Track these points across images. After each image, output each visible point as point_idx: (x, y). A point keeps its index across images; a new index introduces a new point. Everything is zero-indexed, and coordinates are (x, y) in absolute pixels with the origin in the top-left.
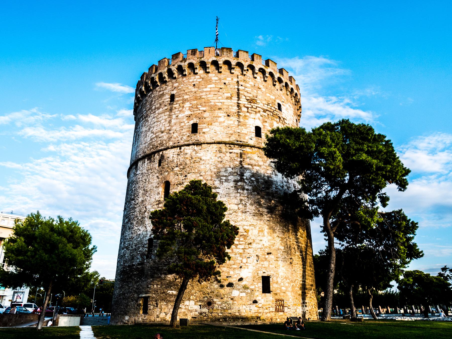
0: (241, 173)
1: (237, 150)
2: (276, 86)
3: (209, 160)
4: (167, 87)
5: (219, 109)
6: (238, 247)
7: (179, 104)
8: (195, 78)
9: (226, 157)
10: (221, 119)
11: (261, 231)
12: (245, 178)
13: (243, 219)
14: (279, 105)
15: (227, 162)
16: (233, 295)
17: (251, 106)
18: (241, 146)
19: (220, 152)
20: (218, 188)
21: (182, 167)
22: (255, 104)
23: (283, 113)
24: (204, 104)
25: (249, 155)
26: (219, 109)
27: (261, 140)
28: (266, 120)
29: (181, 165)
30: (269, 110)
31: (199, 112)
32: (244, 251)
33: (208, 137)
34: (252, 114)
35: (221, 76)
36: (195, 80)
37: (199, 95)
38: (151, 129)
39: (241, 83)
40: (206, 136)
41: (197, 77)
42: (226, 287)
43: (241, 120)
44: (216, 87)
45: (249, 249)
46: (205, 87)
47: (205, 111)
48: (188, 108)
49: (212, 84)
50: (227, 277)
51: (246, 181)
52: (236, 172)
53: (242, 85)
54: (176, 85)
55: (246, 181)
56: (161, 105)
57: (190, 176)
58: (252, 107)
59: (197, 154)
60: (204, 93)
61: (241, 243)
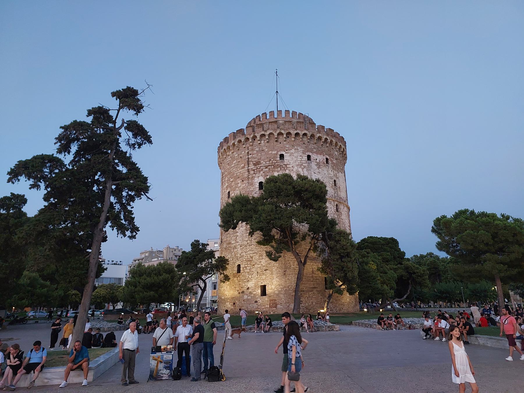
6: (247, 268)
16: (244, 298)
23: (285, 161)
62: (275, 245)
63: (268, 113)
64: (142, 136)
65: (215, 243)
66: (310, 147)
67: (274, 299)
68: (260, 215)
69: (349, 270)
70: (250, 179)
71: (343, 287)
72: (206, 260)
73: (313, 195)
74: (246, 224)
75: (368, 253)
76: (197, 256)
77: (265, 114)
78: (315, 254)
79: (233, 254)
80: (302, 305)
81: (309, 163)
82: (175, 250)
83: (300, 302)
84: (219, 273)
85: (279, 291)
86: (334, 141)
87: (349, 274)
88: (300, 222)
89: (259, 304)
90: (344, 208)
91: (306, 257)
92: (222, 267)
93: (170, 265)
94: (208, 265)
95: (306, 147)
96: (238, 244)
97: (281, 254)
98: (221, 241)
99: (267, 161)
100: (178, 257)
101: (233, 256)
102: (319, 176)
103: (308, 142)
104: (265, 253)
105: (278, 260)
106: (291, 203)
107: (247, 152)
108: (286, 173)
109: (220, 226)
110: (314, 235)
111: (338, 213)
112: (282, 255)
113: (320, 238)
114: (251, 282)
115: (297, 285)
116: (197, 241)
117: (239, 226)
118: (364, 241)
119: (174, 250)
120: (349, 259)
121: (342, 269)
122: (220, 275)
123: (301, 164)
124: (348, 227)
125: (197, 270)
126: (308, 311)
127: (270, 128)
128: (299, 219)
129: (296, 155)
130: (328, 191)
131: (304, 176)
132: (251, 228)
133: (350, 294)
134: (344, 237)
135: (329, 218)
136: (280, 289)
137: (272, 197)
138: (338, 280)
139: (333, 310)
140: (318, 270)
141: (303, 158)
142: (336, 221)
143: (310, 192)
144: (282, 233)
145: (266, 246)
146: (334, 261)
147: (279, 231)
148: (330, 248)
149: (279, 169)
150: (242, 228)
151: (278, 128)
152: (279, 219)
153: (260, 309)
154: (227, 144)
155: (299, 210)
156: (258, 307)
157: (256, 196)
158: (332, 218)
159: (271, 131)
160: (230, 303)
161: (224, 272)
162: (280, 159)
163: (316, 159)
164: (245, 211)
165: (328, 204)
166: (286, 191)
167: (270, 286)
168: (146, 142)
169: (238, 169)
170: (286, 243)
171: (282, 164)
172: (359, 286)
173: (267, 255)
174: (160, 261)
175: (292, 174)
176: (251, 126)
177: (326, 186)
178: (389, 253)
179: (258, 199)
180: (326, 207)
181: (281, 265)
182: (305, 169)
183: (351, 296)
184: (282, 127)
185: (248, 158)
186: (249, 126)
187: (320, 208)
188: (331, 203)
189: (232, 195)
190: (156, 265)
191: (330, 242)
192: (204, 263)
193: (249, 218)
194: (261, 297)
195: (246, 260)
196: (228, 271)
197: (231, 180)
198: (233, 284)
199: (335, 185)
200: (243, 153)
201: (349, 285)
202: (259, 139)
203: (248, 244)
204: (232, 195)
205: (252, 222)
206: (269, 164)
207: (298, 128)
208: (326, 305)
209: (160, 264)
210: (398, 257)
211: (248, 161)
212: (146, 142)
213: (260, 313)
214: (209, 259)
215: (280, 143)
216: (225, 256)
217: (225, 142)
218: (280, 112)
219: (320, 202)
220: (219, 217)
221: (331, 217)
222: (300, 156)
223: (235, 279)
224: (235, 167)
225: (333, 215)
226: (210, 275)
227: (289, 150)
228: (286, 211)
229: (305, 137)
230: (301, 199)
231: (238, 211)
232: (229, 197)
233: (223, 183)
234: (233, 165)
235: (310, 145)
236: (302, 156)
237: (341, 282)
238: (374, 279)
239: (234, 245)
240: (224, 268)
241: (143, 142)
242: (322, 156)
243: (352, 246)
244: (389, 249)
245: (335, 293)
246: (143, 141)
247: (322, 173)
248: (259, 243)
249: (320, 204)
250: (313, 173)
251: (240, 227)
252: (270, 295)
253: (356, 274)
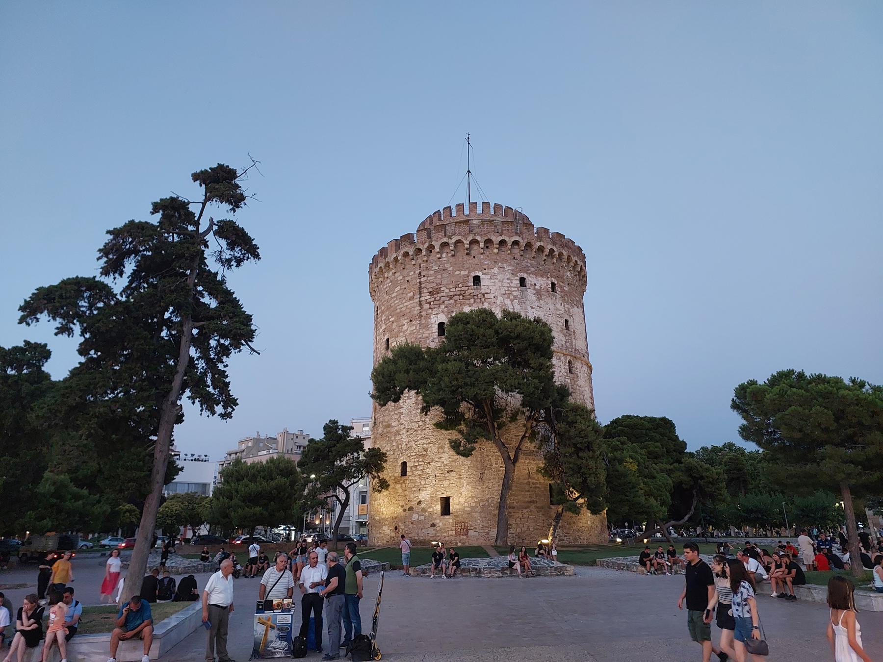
11: (442, 447)
16: (413, 519)
22: (439, 295)
23: (482, 287)
62: (465, 429)
63: (453, 207)
64: (243, 245)
65: (364, 425)
66: (524, 264)
67: (463, 520)
68: (440, 379)
69: (591, 472)
70: (423, 318)
71: (581, 501)
72: (350, 454)
73: (529, 345)
74: (417, 393)
75: (623, 444)
76: (334, 447)
77: (449, 208)
78: (533, 445)
79: (394, 444)
80: (512, 531)
81: (522, 291)
82: (297, 437)
83: (508, 527)
84: (370, 477)
85: (472, 507)
86: (565, 253)
87: (591, 480)
88: (508, 391)
89: (438, 529)
90: (582, 367)
91: (518, 449)
92: (375, 466)
93: (289, 462)
94: (353, 463)
95: (518, 264)
96: (403, 426)
97: (475, 445)
98: (375, 423)
99: (452, 287)
100: (302, 449)
101: (395, 448)
102: (539, 313)
103: (521, 256)
104: (448, 442)
105: (471, 455)
106: (492, 359)
107: (417, 272)
108: (483, 307)
109: (372, 396)
110: (532, 412)
111: (572, 376)
112: (477, 446)
113: (542, 417)
114: (425, 492)
115: (503, 497)
116: (335, 422)
117: (405, 397)
118: (616, 422)
119: (295, 436)
120: (591, 453)
121: (578, 470)
122: (372, 480)
123: (509, 292)
124: (590, 400)
125: (334, 471)
126: (521, 541)
127: (457, 233)
128: (506, 385)
129: (500, 277)
130: (554, 338)
131: (514, 312)
132: (425, 401)
133: (592, 513)
134: (583, 417)
135: (556, 384)
136: (474, 505)
137: (460, 348)
138: (571, 489)
139: (564, 540)
140: (538, 471)
141: (512, 283)
142: (568, 388)
143: (524, 340)
144: (477, 410)
145: (450, 432)
146: (565, 456)
147: (471, 406)
148: (559, 435)
149: (472, 301)
150: (409, 400)
151: (471, 231)
152: (472, 385)
153: (439, 538)
154: (385, 258)
155: (505, 371)
156: (436, 534)
157: (433, 346)
158: (561, 385)
159: (459, 238)
160: (389, 527)
161: (379, 474)
162: (474, 285)
163: (535, 284)
164: (414, 371)
165: (554, 361)
166: (484, 338)
167: (456, 499)
168: (250, 256)
169: (404, 301)
170: (484, 426)
171: (476, 293)
172: (607, 500)
173: (452, 447)
174: (271, 455)
175: (493, 310)
176: (425, 229)
177: (551, 330)
178: (659, 444)
179: (437, 351)
180: (552, 366)
181: (475, 463)
182: (516, 302)
183: (594, 517)
184: (477, 230)
185: (420, 283)
186: (422, 228)
187: (541, 367)
188: (560, 359)
189: (393, 344)
190: (264, 462)
191: (559, 425)
192: (345, 459)
193: (421, 383)
194: (442, 517)
195: (415, 455)
196: (386, 473)
197: (391, 320)
198: (395, 495)
199: (567, 328)
200: (412, 274)
201: (591, 497)
202: (438, 250)
203: (419, 427)
204: (393, 344)
205: (427, 390)
206: (456, 293)
207: (504, 232)
208: (551, 531)
209: (272, 460)
210: (674, 451)
211: (420, 288)
212: (250, 256)
213: (440, 544)
214: (354, 452)
215: (474, 257)
216: (380, 447)
217: (381, 255)
218: (473, 205)
219: (541, 356)
220: (371, 381)
221: (560, 383)
222: (508, 279)
223: (398, 486)
224: (399, 297)
225: (563, 379)
226: (355, 480)
227: (488, 269)
228: (483, 370)
229: (516, 247)
230: (508, 351)
231: (402, 372)
232: (387, 347)
233: (378, 325)
234: (393, 295)
235: (524, 260)
236: (511, 280)
237: (576, 493)
238: (633, 487)
239: (396, 428)
240: (380, 468)
241: (244, 257)
242: (544, 279)
243: (596, 432)
244: (658, 437)
245: (566, 511)
246: (245, 254)
247: (545, 308)
248: (439, 426)
249: (541, 360)
250: (529, 308)
251: (406, 398)
252: (456, 514)
253: (603, 478)
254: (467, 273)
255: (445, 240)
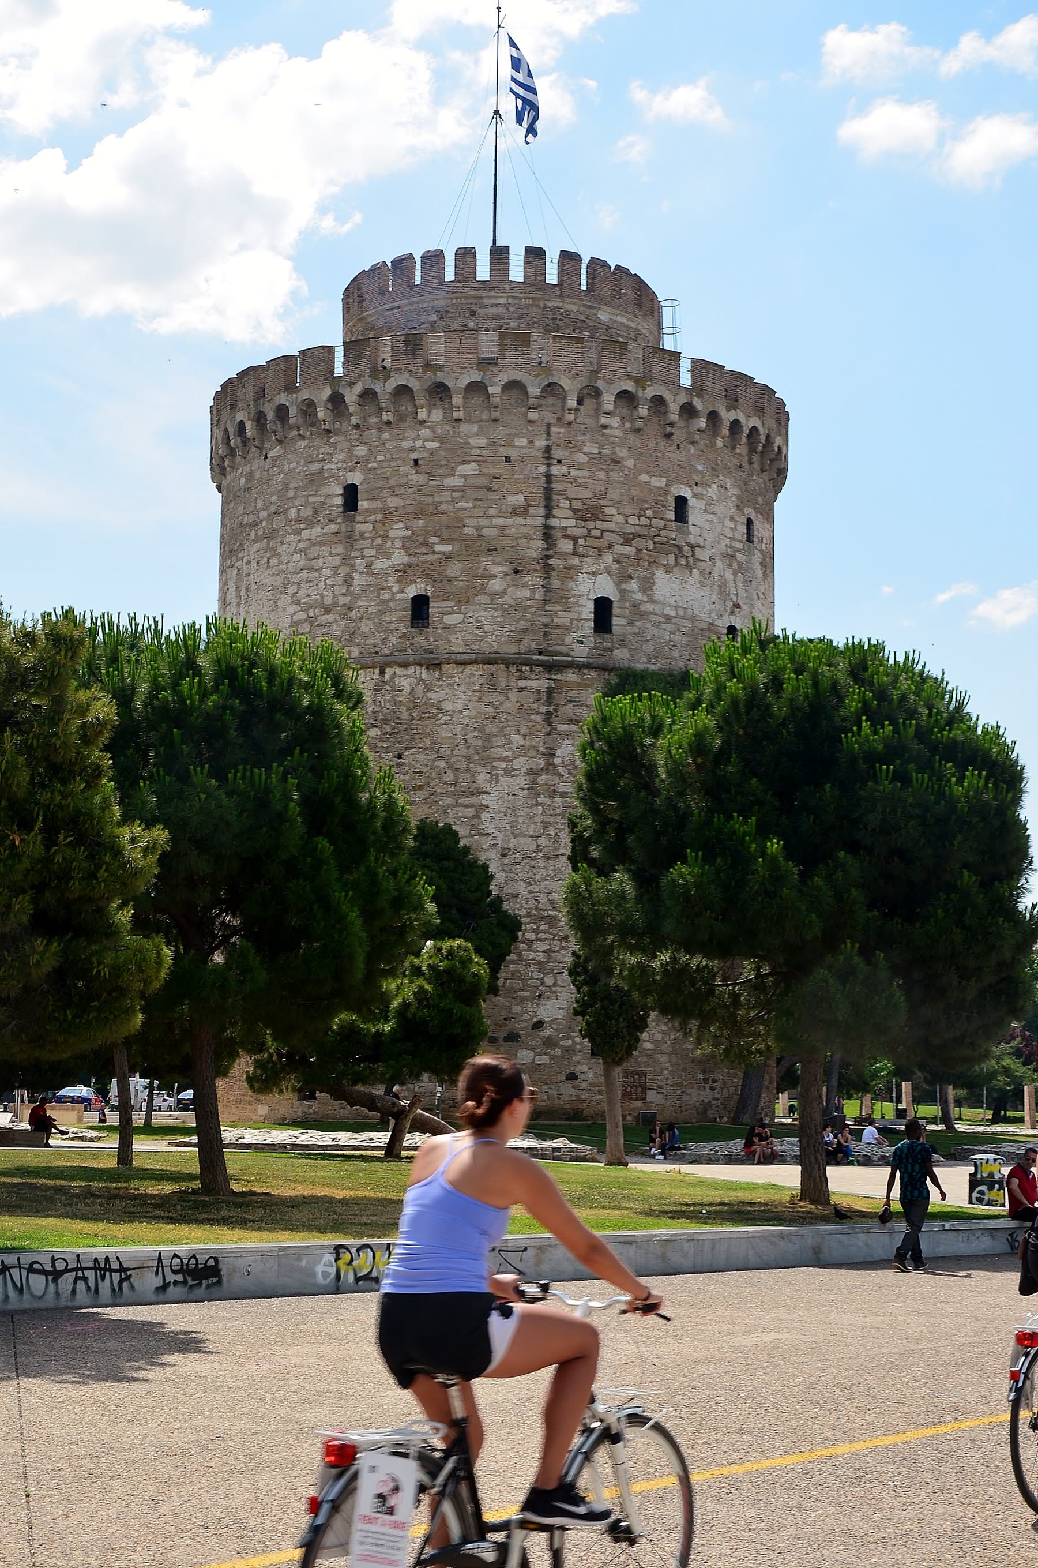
0: (547, 748)
1: (538, 682)
2: (674, 437)
3: (461, 712)
4: (331, 450)
5: (489, 550)
7: (374, 523)
8: (418, 437)
9: (508, 704)
10: (496, 585)
12: (557, 761)
13: (548, 875)
14: (681, 503)
15: (510, 718)
17: (585, 531)
18: (550, 667)
19: (492, 687)
20: (485, 793)
21: (388, 729)
22: (599, 524)
23: (691, 529)
24: (445, 533)
25: (573, 693)
26: (489, 550)
27: (612, 642)
28: (631, 571)
29: (385, 721)
30: (643, 531)
31: (431, 557)
32: (549, 957)
33: (460, 641)
34: (589, 560)
35: (500, 433)
36: (419, 443)
37: (430, 500)
38: (292, 590)
39: (557, 453)
40: (453, 638)
41: (425, 432)
42: (501, 1042)
43: (556, 584)
44: (481, 474)
45: (562, 952)
46: (447, 472)
47: (448, 557)
48: (398, 544)
49: (468, 463)
50: (505, 1019)
51: (560, 769)
52: (534, 747)
53: (559, 462)
54: (361, 451)
55: (560, 769)
56: (316, 512)
57: (412, 757)
58: (589, 535)
59: (430, 695)
60: (446, 496)
61: (542, 936)
254: (663, 485)
255: (629, 386)
